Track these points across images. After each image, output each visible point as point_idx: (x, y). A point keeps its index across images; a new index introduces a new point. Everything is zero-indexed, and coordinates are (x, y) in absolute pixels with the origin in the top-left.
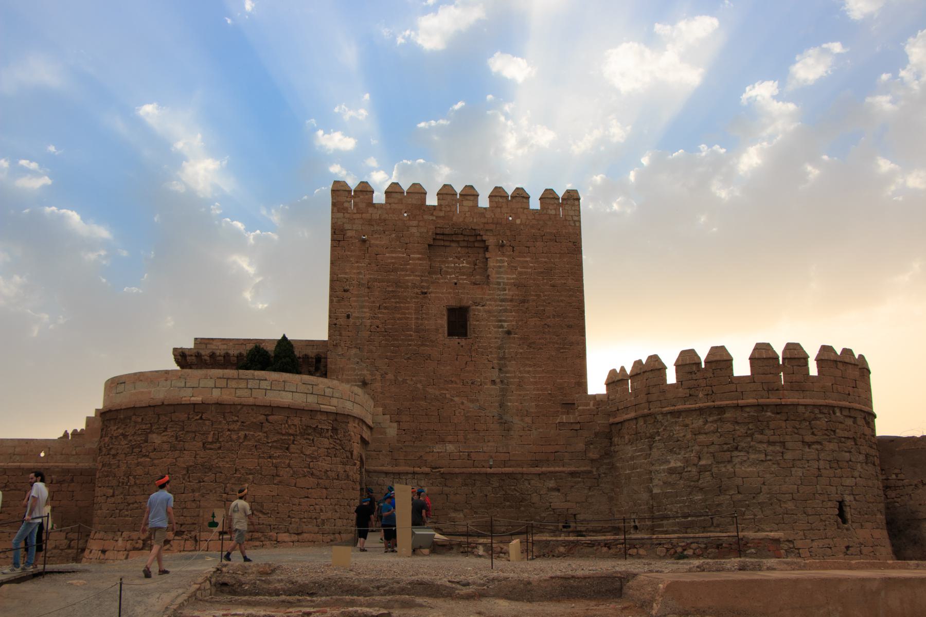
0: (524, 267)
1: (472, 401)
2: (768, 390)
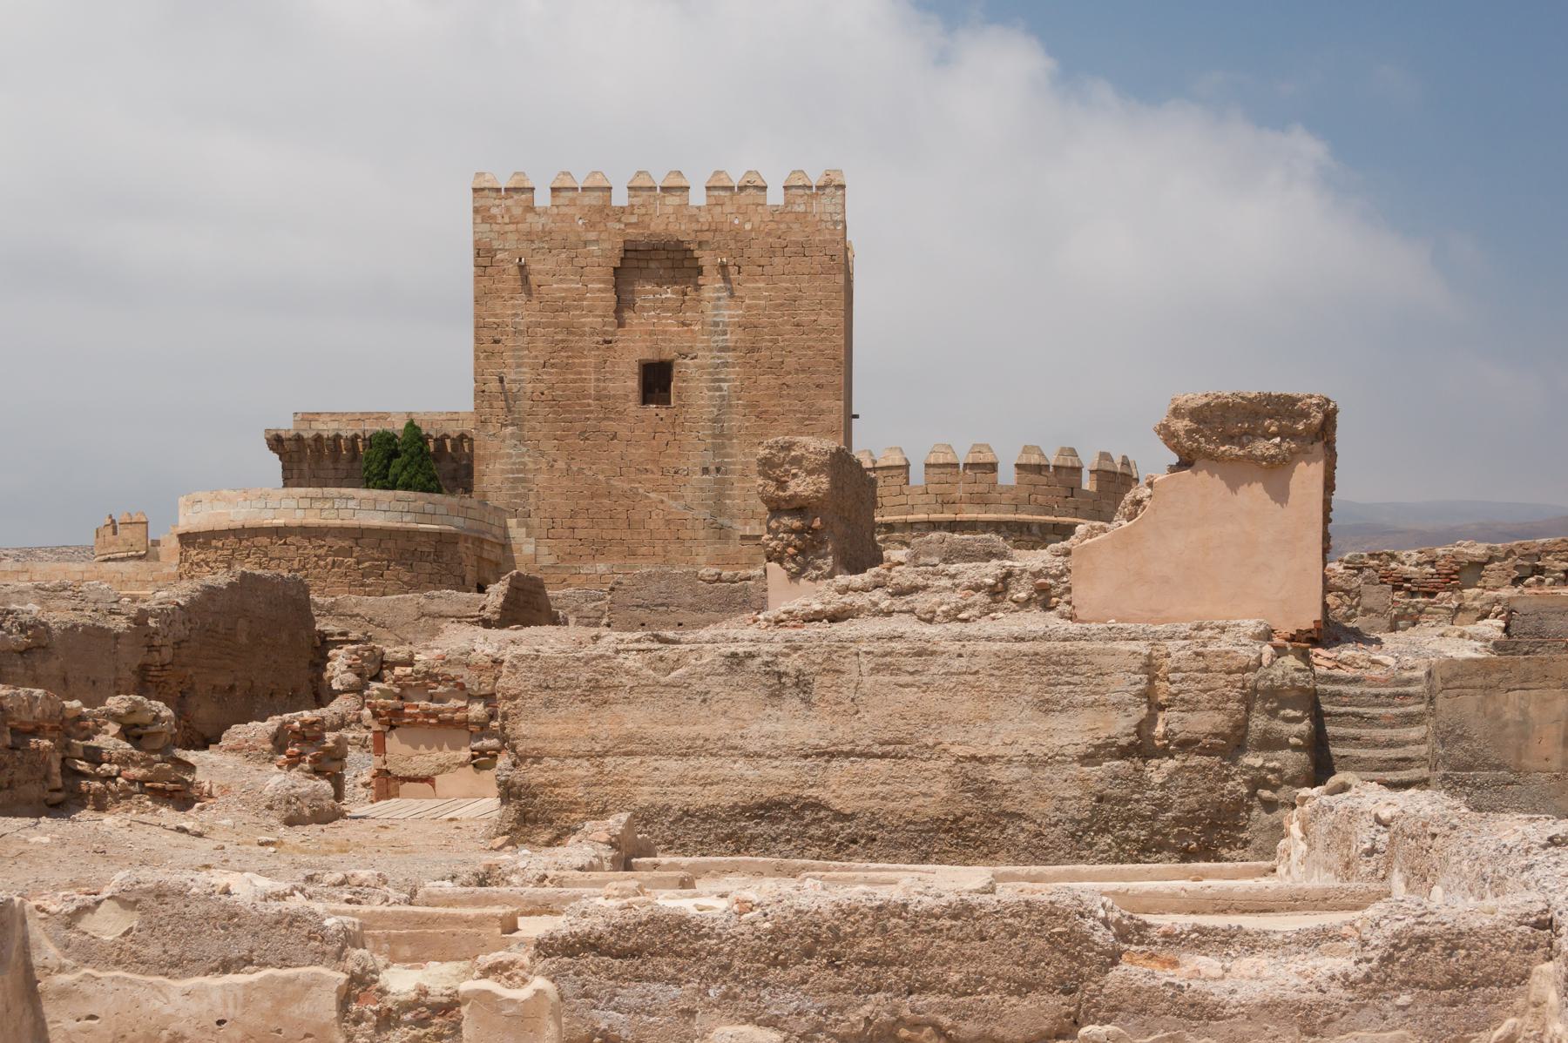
0: (754, 298)
1: (675, 498)
2: (943, 503)
